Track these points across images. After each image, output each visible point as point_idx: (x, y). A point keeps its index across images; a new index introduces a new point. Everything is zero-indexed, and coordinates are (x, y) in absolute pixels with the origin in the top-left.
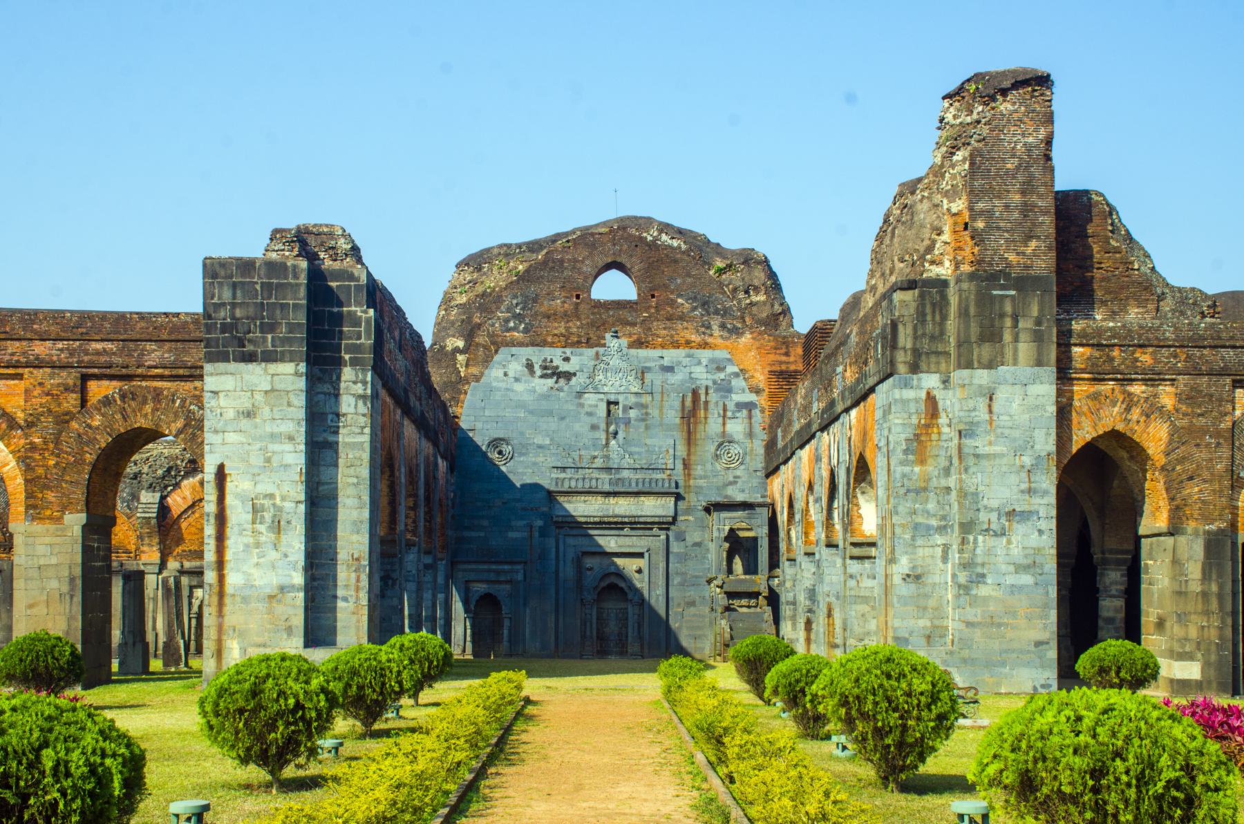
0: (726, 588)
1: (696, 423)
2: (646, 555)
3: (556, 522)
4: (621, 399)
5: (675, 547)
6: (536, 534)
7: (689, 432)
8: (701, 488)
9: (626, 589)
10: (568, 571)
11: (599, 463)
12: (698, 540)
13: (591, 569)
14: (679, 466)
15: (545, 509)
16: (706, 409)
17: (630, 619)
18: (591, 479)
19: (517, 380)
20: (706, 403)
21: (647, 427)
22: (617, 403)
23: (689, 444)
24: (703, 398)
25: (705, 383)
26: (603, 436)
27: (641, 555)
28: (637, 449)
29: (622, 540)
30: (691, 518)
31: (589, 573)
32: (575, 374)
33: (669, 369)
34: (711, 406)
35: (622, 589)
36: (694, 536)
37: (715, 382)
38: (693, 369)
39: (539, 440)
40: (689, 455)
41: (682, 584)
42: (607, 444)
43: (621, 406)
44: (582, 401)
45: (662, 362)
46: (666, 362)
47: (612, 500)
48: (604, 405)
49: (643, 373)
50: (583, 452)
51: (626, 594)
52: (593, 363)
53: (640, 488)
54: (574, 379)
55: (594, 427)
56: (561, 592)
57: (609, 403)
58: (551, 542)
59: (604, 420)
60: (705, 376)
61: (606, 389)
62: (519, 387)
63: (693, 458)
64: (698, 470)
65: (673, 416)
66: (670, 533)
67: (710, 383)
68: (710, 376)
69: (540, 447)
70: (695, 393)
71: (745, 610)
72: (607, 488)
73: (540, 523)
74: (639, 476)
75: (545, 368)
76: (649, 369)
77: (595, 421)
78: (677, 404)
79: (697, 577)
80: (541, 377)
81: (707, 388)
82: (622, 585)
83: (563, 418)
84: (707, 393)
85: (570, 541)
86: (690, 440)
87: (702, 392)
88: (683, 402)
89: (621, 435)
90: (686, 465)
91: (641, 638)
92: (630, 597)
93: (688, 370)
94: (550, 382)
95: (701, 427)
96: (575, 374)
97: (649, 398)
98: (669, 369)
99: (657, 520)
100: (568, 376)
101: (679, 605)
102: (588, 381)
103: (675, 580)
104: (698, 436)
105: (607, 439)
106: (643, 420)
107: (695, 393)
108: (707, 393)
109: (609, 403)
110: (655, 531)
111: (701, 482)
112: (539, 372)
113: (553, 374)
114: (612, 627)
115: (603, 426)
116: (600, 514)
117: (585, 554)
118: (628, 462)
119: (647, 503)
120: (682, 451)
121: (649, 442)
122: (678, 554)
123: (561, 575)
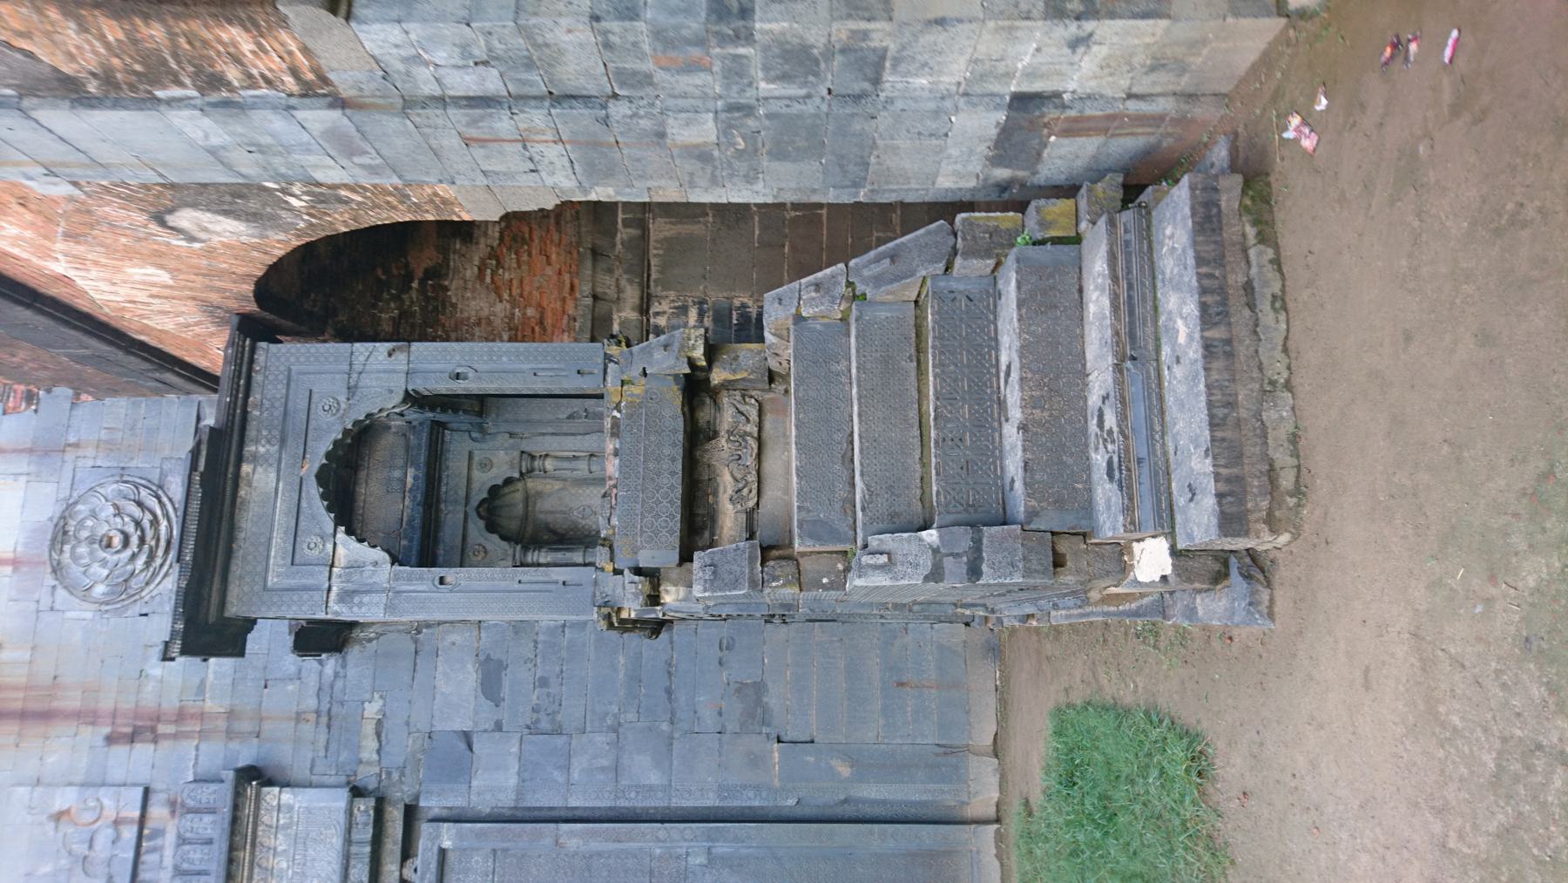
0: (661, 554)
5: (497, 780)
12: (470, 677)
14: (140, 760)
23: (46, 716)
30: (372, 709)
36: (454, 693)
40: (87, 716)
63: (106, 703)
66: (431, 803)
71: (785, 462)
79: (635, 678)
101: (756, 761)
103: (647, 779)
120: (66, 749)
122: (528, 770)
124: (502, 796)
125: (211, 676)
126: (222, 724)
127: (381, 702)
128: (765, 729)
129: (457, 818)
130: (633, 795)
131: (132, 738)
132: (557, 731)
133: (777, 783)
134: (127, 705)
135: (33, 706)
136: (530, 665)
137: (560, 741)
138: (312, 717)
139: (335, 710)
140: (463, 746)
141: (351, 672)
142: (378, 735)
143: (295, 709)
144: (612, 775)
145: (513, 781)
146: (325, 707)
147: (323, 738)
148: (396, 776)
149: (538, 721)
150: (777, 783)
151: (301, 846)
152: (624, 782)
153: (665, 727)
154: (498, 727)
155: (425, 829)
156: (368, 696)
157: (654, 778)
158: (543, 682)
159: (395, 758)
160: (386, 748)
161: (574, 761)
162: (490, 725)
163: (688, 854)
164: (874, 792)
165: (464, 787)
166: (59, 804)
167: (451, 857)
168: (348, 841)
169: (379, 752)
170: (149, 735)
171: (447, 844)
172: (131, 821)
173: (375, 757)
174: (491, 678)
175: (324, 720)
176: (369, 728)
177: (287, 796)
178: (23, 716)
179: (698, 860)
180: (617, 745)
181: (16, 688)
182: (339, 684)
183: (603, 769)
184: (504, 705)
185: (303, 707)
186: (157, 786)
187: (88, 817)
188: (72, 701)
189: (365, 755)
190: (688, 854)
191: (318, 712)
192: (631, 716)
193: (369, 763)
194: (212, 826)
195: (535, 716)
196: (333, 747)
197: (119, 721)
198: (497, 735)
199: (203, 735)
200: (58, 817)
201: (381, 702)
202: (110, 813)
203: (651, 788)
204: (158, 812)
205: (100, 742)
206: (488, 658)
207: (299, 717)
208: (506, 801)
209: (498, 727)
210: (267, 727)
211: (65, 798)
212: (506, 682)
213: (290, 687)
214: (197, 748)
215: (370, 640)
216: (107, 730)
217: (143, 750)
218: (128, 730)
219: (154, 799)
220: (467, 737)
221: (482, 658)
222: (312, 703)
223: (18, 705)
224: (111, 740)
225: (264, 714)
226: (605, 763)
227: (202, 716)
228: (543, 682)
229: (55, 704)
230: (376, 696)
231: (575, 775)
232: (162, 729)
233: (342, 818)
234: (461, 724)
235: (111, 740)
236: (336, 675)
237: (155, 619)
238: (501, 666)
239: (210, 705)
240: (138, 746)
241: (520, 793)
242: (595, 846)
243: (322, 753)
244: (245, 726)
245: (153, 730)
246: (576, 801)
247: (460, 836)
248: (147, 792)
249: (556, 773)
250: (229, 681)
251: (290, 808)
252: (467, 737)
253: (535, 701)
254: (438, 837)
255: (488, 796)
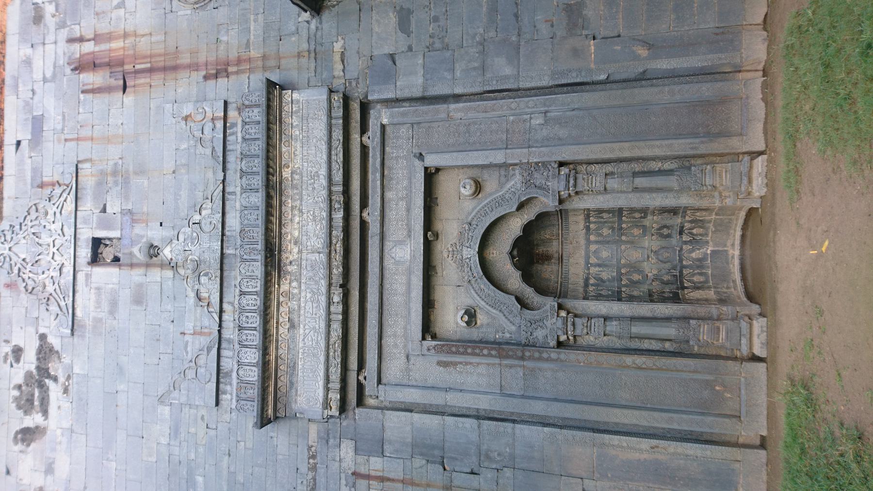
1: (135, 58)
2: (432, 161)
3: (343, 409)
4: (86, 234)
5: (411, 82)
6: (376, 464)
7: (151, 70)
8: (267, 27)
9: (529, 215)
10: (477, 381)
11: (210, 288)
12: (392, 19)
13: (471, 315)
14: (222, 88)
15: (313, 429)
16: (110, 37)
17: (621, 201)
18: (242, 310)
19: (49, 470)
20: (97, 38)
21: (141, 171)
22: (97, 243)
23: (175, 68)
24: (89, 47)
25: (62, 46)
26: (156, 275)
27: (431, 177)
28: (184, 194)
29: (395, 230)
30: (338, 47)
31: (481, 318)
32: (43, 337)
33: (37, 124)
34: (103, 27)
35: (528, 228)
37: (62, 25)
38: (38, 75)
39: (160, 432)
40: (194, 67)
41: (514, 52)
42: (172, 266)
43: (100, 234)
44: (89, 323)
45: (24, 144)
46: (25, 136)
47: (291, 253)
48: (99, 272)
49: (42, 186)
50: (189, 327)
51: (542, 217)
52: (24, 296)
53: (258, 181)
54: (54, 341)
55: (139, 299)
56: (538, 408)
57: (95, 259)
58: (397, 425)
59: (125, 271)
60: (50, 48)
61: (68, 269)
62: (63, 467)
63: (202, 59)
64: (231, 42)
65: (123, 111)
67: (64, 34)
68: (50, 38)
69: (175, 432)
70: (81, 66)
72: (258, 269)
73: (347, 450)
74: (235, 185)
75: (30, 401)
76: (37, 171)
77: (125, 295)
78: (99, 102)
80: (45, 412)
81: (71, 41)
82: (515, 227)
83: (120, 370)
84: (81, 40)
85: (394, 369)
86: (166, 67)
87: (78, 50)
88: (93, 91)
89: (155, 234)
90: (219, 71)
91: (685, 163)
92: (549, 203)
93: (38, 87)
94: (54, 390)
95: (144, 45)
96: (43, 337)
97: (85, 167)
98: (37, 124)
99: (338, 134)
100: (45, 352)
101: (576, 53)
102: (54, 308)
103: (502, 70)
104: (159, 49)
105: (162, 266)
106: (126, 182)
107: (81, 66)
108: (81, 40)
109: (95, 259)
110: (372, 140)
111: (255, 29)
112: (35, 419)
113: (42, 386)
114: (645, 255)
115: (137, 275)
116: (324, 283)
117: (428, 329)
118: (210, 215)
119: (297, 163)
120: (187, 85)
121: (169, 166)
123: (484, 403)
124: (414, 90)
125: (252, 37)
126: (260, 63)
127: (342, 42)
128: (585, 32)
129: (389, 103)
130: (494, 82)
131: (216, 76)
132: (446, 47)
133: (592, 66)
134: (212, 58)
135: (169, 63)
136: (426, 9)
137: (448, 54)
138: (306, 54)
139: (319, 48)
140: (390, 62)
141: (325, 26)
142: (343, 61)
143: (297, 51)
144: (480, 72)
145: (420, 80)
146: (312, 47)
147: (313, 65)
148: (354, 84)
149: (434, 43)
150: (592, 66)
151: (305, 122)
152: (488, 75)
153: (514, 38)
154: (410, 49)
155: (373, 113)
156: (335, 39)
157: (508, 71)
158: (436, 19)
159: (352, 73)
160: (347, 68)
161: (457, 66)
162: (405, 49)
163: (531, 118)
164: (664, 64)
165: (393, 86)
166: (186, 112)
167: (388, 129)
168: (330, 117)
169: (343, 71)
170: (225, 74)
171: (385, 121)
172: (220, 119)
173: (342, 73)
174: (404, 25)
175: (313, 55)
176: (337, 58)
177: (296, 95)
178: (165, 69)
179: (538, 121)
180: (483, 52)
181: (160, 55)
182: (319, 33)
183: (475, 68)
184: (413, 35)
185: (301, 49)
186: (229, 100)
187: (199, 117)
188: (185, 59)
189: (336, 73)
190: (531, 118)
191: (309, 51)
192: (492, 34)
193: (339, 78)
194: (258, 115)
195: (431, 40)
196: (319, 70)
197: (209, 67)
198: (409, 53)
199: (251, 70)
200: (186, 118)
201: (342, 42)
202: (209, 115)
203: (507, 77)
204: (232, 114)
205: (201, 79)
206: (402, 8)
207: (299, 55)
208: (417, 93)
209: (410, 49)
210: (283, 62)
211: (188, 109)
212: (413, 21)
213: (293, 39)
214: (249, 78)
215: (334, 6)
216: (204, 73)
217: (222, 81)
218: (214, 72)
219: (230, 107)
220: (392, 57)
221: (398, 8)
222: (305, 46)
223: (161, 64)
224: (206, 78)
225: (281, 55)
226: (476, 65)
227: (249, 60)
228: (436, 19)
229: (178, 62)
230: (340, 38)
231: (458, 74)
232: (230, 69)
233: (325, 104)
234: (388, 50)
235: (206, 78)
236: (317, 28)
237: (221, 9)
238: (410, 12)
239: (254, 53)
240: (219, 80)
241: (425, 89)
242: (470, 115)
243: (313, 74)
244: (272, 63)
245: (226, 70)
246: (458, 90)
247: (392, 116)
248: (226, 103)
249: (446, 73)
250: (261, 39)
251: (298, 101)
252: (392, 57)
253: (431, 31)
254: (380, 116)
255: (407, 91)
